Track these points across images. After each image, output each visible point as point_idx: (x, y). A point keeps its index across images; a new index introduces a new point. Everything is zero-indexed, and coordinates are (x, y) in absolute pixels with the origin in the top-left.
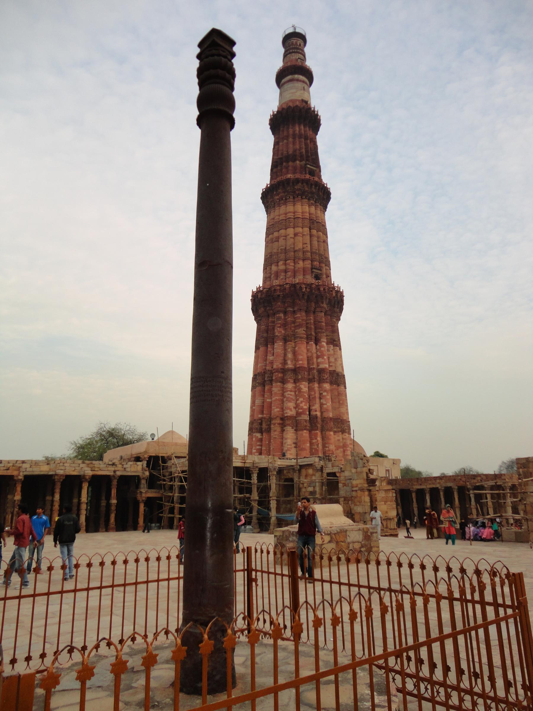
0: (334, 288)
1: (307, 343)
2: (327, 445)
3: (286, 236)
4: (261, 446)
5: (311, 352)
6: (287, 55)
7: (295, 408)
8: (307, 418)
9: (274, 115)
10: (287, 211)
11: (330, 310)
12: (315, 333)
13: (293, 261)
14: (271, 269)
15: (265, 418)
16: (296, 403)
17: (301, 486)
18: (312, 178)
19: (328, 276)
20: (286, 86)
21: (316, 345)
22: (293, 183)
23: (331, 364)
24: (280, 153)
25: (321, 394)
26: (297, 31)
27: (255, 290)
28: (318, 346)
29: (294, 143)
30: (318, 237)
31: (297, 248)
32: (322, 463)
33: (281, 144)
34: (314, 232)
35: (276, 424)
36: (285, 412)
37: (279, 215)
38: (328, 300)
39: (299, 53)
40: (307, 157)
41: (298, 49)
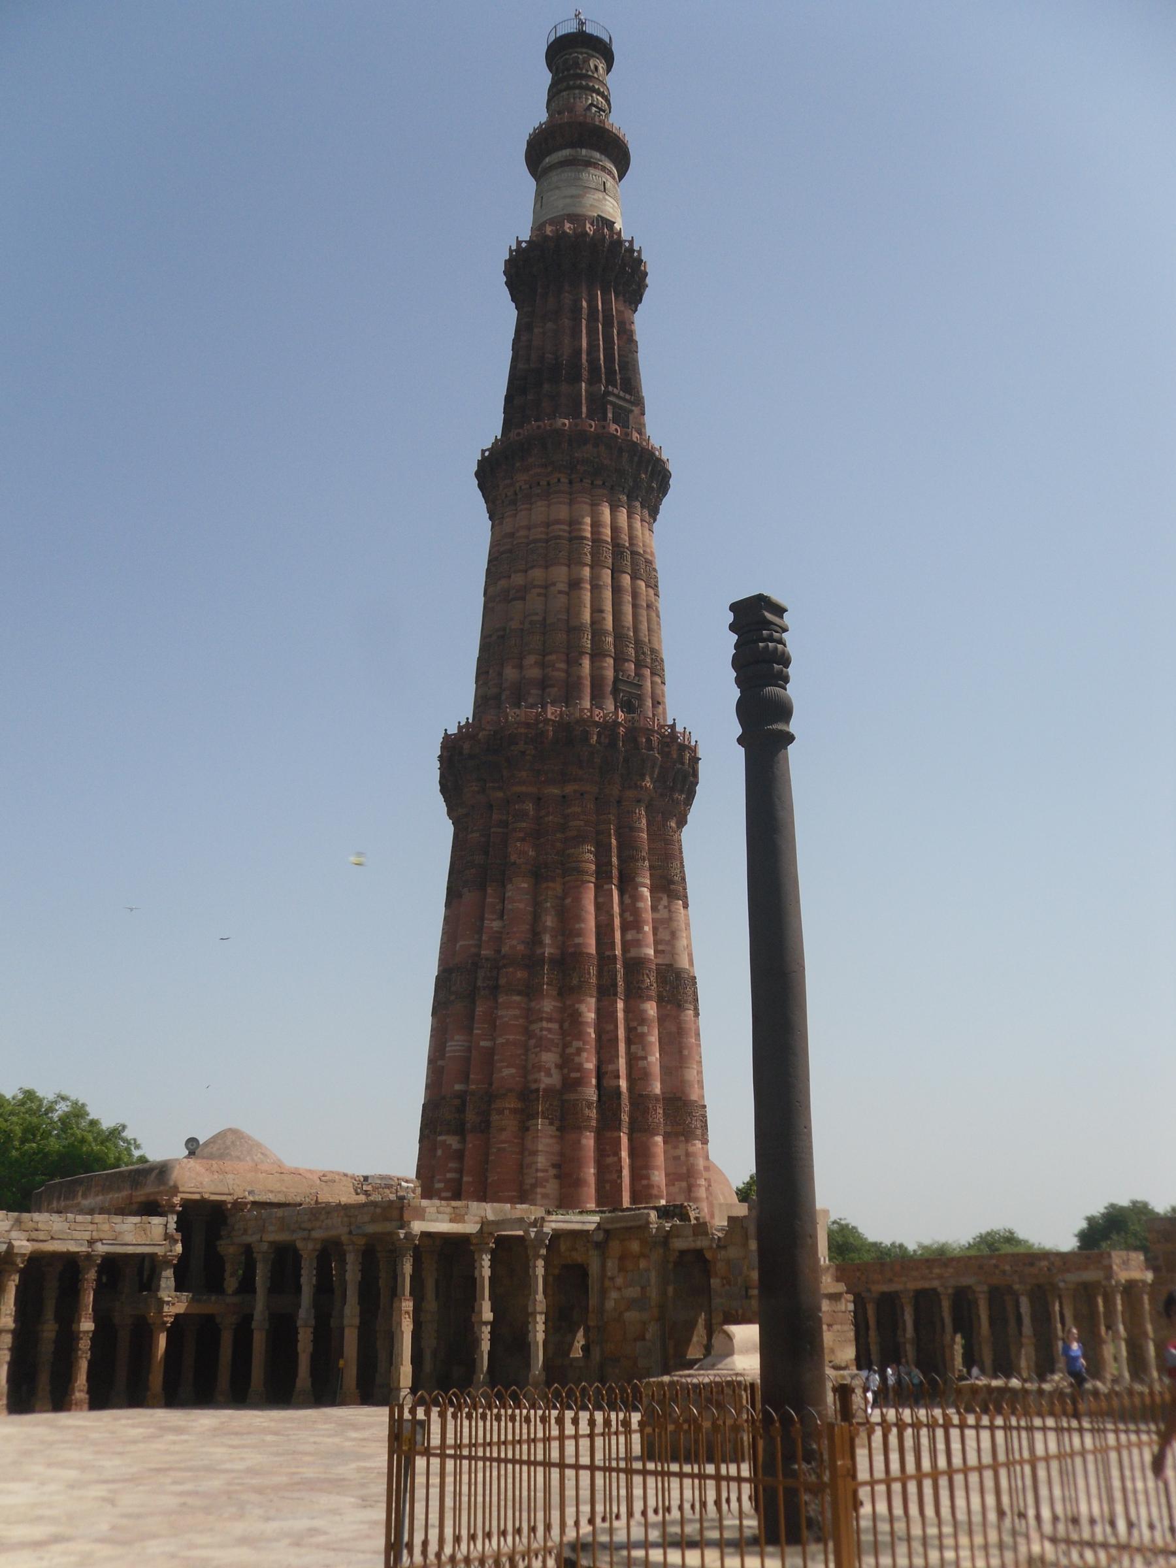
0: (673, 735)
1: (598, 887)
2: (644, 1172)
3: (546, 587)
4: (460, 1171)
6: (561, 91)
7: (557, 1066)
8: (591, 1093)
9: (519, 250)
12: (619, 857)
14: (500, 674)
16: (563, 1055)
17: (607, 1283)
19: (657, 703)
20: (554, 177)
23: (660, 948)
25: (629, 1030)
26: (589, 29)
27: (453, 730)
28: (626, 897)
29: (576, 334)
30: (635, 595)
32: (668, 1226)
33: (536, 330)
35: (507, 1112)
36: (530, 1078)
37: (529, 528)
40: (610, 372)
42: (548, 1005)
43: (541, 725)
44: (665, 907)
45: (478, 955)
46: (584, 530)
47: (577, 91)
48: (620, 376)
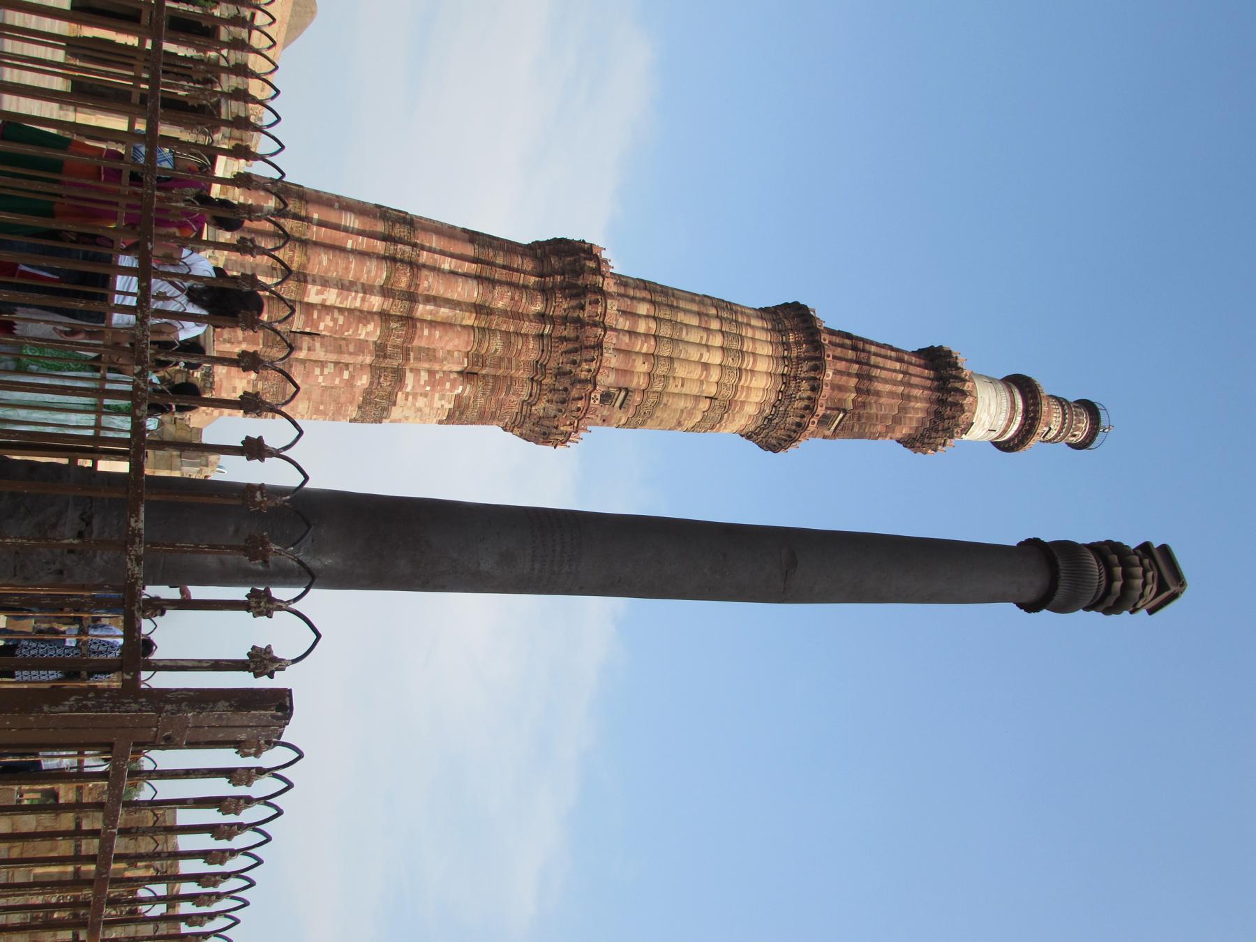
5: (446, 359)
6: (1063, 407)
7: (324, 300)
8: (298, 323)
10: (759, 359)
13: (651, 351)
14: (643, 300)
15: (308, 227)
18: (815, 419)
21: (460, 373)
22: (815, 379)
23: (410, 398)
24: (880, 361)
25: (347, 365)
27: (604, 255)
30: (690, 414)
31: (676, 365)
33: (897, 366)
34: (704, 405)
37: (753, 339)
38: (552, 413)
39: (1059, 432)
41: (1068, 430)
42: (376, 302)
45: (423, 248)
48: (853, 422)
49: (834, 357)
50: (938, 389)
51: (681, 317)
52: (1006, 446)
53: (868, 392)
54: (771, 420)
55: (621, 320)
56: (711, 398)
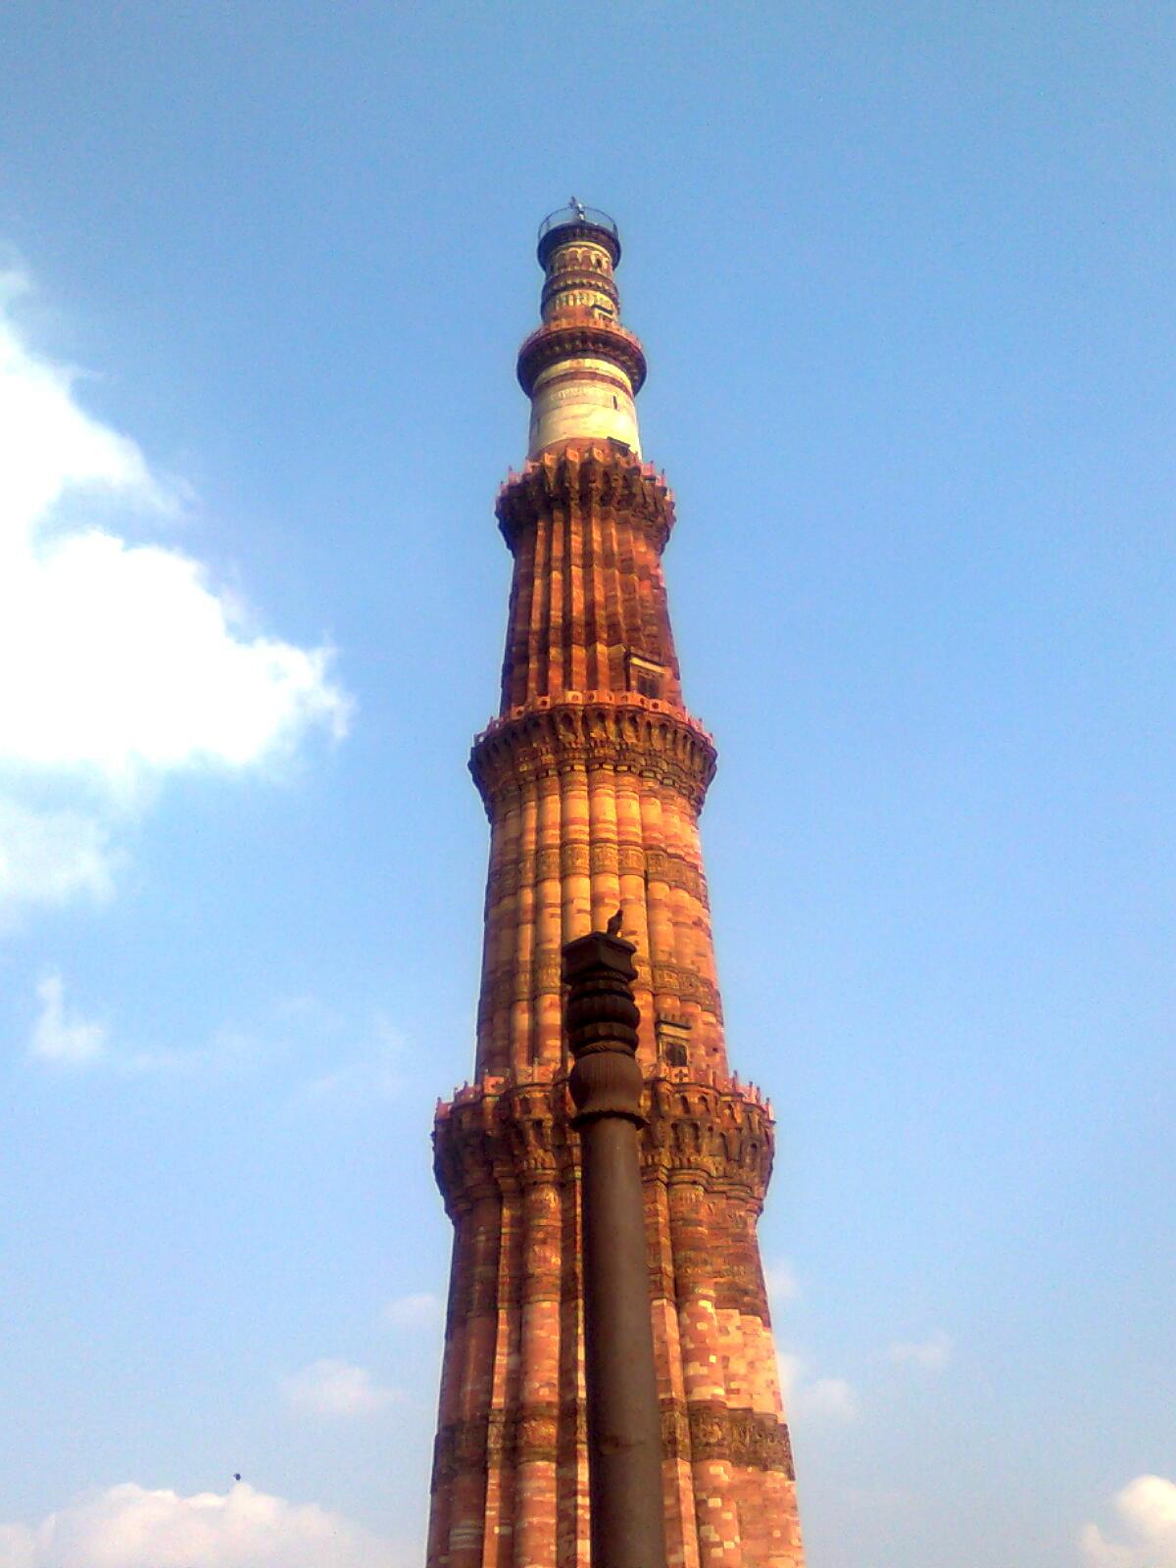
9: (511, 487)
11: (725, 1176)
18: (649, 704)
21: (679, 1308)
22: (585, 719)
23: (734, 1385)
24: (536, 614)
25: (699, 1504)
27: (449, 1098)
29: (588, 584)
30: (677, 909)
33: (538, 582)
34: (661, 890)
38: (718, 1141)
39: (597, 288)
41: (593, 275)
43: (560, 1086)
44: (738, 1328)
45: (489, 1404)
46: (608, 831)
47: (576, 292)
48: (643, 631)
49: (544, 692)
50: (565, 507)
51: (526, 956)
52: (636, 366)
53: (590, 624)
54: (666, 776)
55: (547, 1054)
56: (647, 881)
